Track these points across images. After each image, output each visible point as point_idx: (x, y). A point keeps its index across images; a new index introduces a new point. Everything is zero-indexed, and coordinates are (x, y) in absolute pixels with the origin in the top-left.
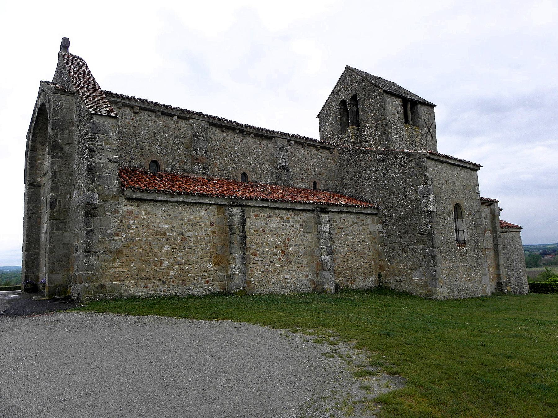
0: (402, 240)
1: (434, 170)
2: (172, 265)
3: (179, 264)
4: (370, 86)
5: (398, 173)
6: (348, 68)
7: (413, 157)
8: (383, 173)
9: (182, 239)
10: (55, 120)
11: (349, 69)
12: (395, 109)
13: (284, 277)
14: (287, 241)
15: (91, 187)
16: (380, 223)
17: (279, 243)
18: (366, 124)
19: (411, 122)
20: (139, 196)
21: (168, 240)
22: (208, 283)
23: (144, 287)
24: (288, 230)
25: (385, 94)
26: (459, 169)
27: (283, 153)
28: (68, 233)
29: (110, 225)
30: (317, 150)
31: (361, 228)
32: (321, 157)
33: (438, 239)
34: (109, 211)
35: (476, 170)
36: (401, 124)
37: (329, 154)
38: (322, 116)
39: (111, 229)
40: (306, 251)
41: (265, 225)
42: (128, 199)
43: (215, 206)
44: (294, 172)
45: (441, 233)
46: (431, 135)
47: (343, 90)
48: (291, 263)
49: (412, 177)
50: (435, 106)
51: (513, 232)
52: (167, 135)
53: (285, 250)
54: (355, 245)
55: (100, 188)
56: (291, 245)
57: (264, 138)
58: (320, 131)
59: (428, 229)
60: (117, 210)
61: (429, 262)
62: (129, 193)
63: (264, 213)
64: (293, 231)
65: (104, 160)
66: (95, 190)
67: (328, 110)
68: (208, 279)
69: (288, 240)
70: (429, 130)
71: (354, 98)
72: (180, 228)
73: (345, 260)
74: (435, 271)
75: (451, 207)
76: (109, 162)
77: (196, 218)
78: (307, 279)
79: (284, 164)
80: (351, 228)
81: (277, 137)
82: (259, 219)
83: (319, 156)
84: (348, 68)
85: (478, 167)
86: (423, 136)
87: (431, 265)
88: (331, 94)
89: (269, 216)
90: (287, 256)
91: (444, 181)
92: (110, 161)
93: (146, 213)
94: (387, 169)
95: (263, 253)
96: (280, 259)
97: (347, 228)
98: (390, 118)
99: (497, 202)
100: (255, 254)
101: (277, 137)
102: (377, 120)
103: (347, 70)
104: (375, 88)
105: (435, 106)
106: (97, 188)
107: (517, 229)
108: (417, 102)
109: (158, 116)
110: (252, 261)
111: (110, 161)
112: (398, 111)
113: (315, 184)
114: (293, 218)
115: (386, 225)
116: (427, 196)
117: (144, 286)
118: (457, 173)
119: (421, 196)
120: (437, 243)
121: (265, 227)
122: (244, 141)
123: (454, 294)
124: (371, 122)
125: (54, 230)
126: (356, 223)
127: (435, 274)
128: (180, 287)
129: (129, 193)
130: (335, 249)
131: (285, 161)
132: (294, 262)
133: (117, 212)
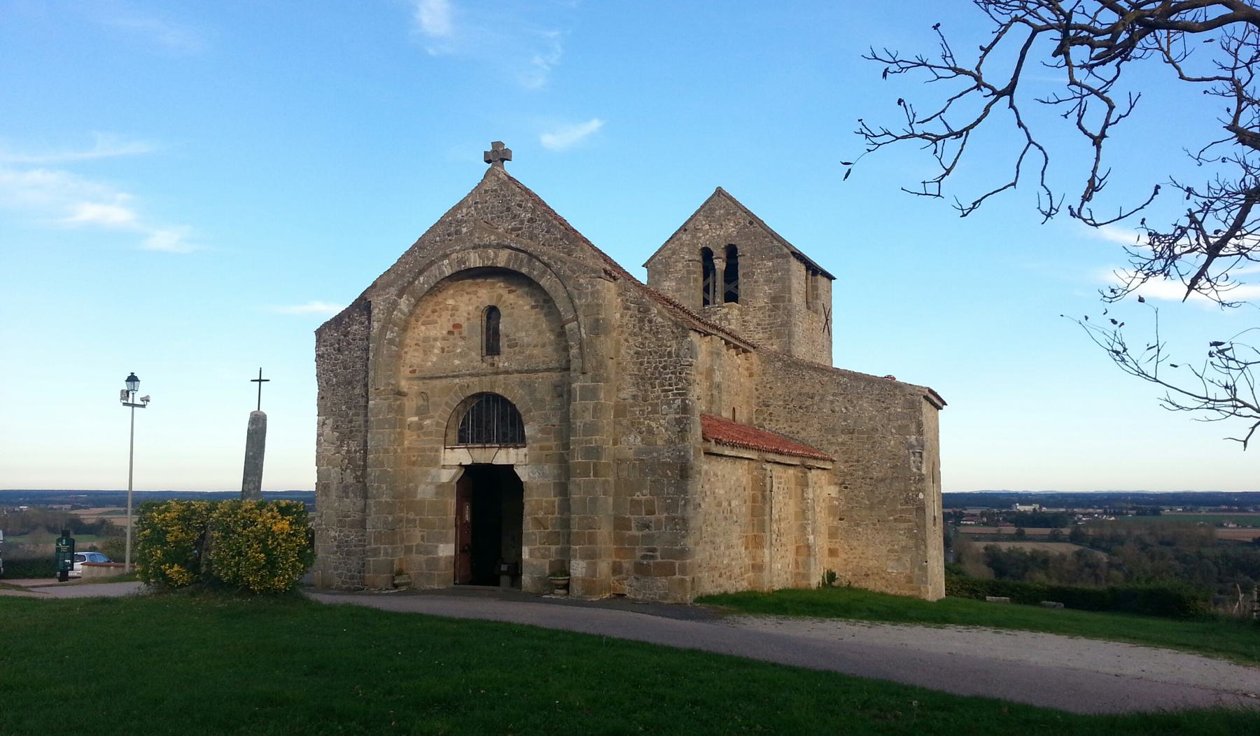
0: (873, 513)
4: (765, 237)
6: (719, 192)
8: (846, 408)
11: (723, 194)
16: (836, 484)
18: (751, 301)
25: (792, 257)
36: (804, 310)
42: (708, 453)
47: (708, 230)
50: (835, 279)
59: (920, 500)
61: (917, 547)
67: (670, 258)
74: (926, 562)
84: (719, 192)
88: (680, 230)
94: (852, 403)
103: (719, 196)
104: (775, 242)
105: (835, 279)
115: (846, 488)
119: (911, 451)
124: (762, 301)
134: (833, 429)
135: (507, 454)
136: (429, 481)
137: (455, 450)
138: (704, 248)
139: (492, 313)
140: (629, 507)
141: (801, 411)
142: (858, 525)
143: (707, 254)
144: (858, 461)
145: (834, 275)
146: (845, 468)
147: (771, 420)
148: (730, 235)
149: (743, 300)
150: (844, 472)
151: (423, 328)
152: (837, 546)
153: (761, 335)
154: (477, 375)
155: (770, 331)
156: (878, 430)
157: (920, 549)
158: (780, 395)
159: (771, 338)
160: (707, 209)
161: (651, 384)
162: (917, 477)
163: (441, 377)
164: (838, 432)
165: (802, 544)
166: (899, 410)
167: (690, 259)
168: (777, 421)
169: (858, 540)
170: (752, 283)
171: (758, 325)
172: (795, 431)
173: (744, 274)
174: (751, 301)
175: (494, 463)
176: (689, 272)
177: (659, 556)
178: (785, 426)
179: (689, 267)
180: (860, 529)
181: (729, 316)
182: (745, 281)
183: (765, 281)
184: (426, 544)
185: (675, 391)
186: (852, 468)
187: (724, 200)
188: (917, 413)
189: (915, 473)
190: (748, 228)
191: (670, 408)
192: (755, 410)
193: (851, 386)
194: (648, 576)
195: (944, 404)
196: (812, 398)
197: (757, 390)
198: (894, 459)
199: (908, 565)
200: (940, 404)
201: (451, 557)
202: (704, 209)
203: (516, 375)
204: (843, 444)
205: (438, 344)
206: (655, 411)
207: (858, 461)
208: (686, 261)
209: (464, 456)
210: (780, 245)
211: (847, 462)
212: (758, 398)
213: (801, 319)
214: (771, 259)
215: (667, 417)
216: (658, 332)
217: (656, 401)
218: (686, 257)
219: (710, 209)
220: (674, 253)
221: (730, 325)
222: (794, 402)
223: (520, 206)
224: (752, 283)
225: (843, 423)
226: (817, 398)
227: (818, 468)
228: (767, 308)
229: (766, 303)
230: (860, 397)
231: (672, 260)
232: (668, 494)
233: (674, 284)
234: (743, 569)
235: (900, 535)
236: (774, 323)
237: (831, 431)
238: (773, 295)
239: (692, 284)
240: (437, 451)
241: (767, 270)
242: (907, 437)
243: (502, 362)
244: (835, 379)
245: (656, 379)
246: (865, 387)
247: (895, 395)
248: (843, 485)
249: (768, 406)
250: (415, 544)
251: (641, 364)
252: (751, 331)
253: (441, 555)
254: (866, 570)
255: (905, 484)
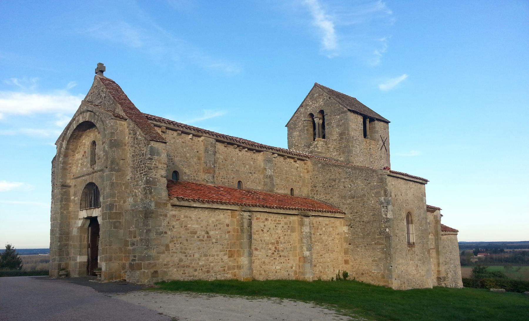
0: (364, 240)
1: (392, 185)
2: (201, 256)
3: (206, 255)
5: (363, 185)
6: (316, 85)
7: (376, 173)
8: (350, 185)
9: (208, 237)
10: (113, 141)
12: (357, 125)
13: (275, 268)
14: (279, 240)
15: (150, 196)
16: (347, 225)
17: (273, 241)
18: (331, 137)
19: (369, 136)
20: (183, 203)
21: (198, 237)
22: (224, 271)
23: (182, 273)
24: (279, 231)
26: (411, 184)
27: (270, 164)
28: (122, 230)
29: (161, 226)
30: (295, 162)
31: (331, 229)
32: (298, 167)
33: (395, 241)
34: (161, 215)
35: (424, 184)
37: (304, 165)
38: (291, 126)
39: (161, 229)
40: (291, 248)
41: (262, 226)
42: (173, 205)
43: (230, 211)
44: (277, 181)
45: (396, 236)
46: (386, 148)
47: (311, 105)
48: (281, 257)
49: (375, 189)
51: (451, 235)
52: (185, 150)
53: (277, 247)
54: (327, 243)
55: (155, 197)
56: (281, 242)
57: (255, 151)
58: (288, 138)
60: (166, 214)
61: (386, 258)
62: (175, 201)
63: (263, 216)
64: (283, 231)
65: (158, 176)
66: (152, 199)
67: (296, 121)
68: (224, 268)
69: (279, 238)
70: (384, 144)
71: (322, 112)
72: (207, 228)
73: (319, 255)
74: (392, 267)
75: (404, 215)
76: (161, 177)
77: (217, 220)
78: (292, 270)
79: (270, 174)
80: (324, 229)
81: (265, 151)
82: (260, 221)
83: (296, 166)
84: (316, 85)
85: (424, 182)
86: (379, 149)
87: (388, 261)
88: (300, 107)
89: (267, 219)
90: (278, 251)
91: (399, 194)
92: (162, 176)
93: (185, 217)
94: (353, 182)
95: (262, 248)
96: (273, 254)
97: (322, 229)
98: (352, 133)
99: (439, 209)
100: (256, 249)
101: (265, 151)
102: (341, 134)
104: (341, 106)
105: (390, 122)
106: (153, 197)
107: (455, 232)
108: (375, 119)
109: (179, 135)
110: (254, 255)
111: (162, 176)
112: (359, 127)
113: (292, 189)
114: (283, 221)
115: (351, 227)
116: (387, 206)
117: (183, 272)
118: (410, 187)
119: (382, 206)
120: (393, 245)
121: (264, 228)
122: (240, 154)
123: (405, 285)
124: (335, 136)
125: (112, 228)
126: (328, 225)
127: (391, 268)
128: (206, 274)
129: (175, 201)
130: (312, 246)
131: (271, 171)
132: (283, 256)
133: (166, 216)
134: (345, 196)
135: (96, 211)
136: (76, 226)
137: (83, 211)
138: (310, 114)
139: (94, 143)
140: (128, 234)
141: (330, 188)
142: (357, 247)
143: (311, 115)
144: (357, 213)
145: (389, 120)
146: (351, 216)
147: (317, 194)
148: (321, 106)
149: (327, 137)
150: (351, 219)
151: (77, 155)
152: (348, 259)
153: (336, 153)
154: (88, 174)
155: (340, 151)
156: (366, 195)
157: (388, 260)
158: (321, 181)
159: (340, 154)
160: (311, 95)
161: (137, 170)
162: (385, 220)
163: (79, 177)
164: (347, 198)
165: (301, 256)
166: (375, 184)
167: (305, 120)
168: (320, 194)
169: (358, 255)
170: (331, 128)
171: (334, 148)
172: (328, 199)
173: (327, 124)
174: (331, 137)
175: (93, 216)
176: (304, 126)
177: (137, 259)
178: (324, 196)
179: (304, 124)
180: (359, 249)
181: (318, 145)
182: (328, 127)
183: (337, 126)
184: (75, 256)
185: (144, 173)
186: (354, 217)
187: (318, 89)
188: (384, 185)
189: (384, 218)
190: (328, 100)
191: (142, 182)
192: (310, 190)
193: (352, 173)
194: (133, 270)
195: (427, 181)
196: (335, 181)
197: (311, 179)
198: (374, 210)
199: (382, 268)
200: (424, 182)
201: (84, 262)
202: (309, 95)
203: (99, 173)
204: (350, 204)
205: (80, 162)
206: (137, 185)
207: (357, 213)
208: (303, 121)
209: (84, 214)
210: (342, 107)
211: (351, 213)
212: (312, 183)
213: (358, 143)
214: (339, 115)
215: (141, 186)
216: (139, 144)
217: (138, 179)
218: (303, 119)
219: (312, 94)
220: (298, 118)
221: (318, 149)
222: (327, 184)
223: (102, 91)
224: (331, 128)
225: (349, 193)
226: (337, 181)
227: (313, 216)
228: (338, 139)
229: (337, 137)
230: (356, 179)
231: (297, 121)
232: (141, 227)
233: (298, 133)
234: (226, 269)
235: (378, 252)
236: (341, 147)
237: (344, 197)
238: (340, 133)
239: (305, 132)
240: (78, 212)
241: (337, 120)
242: (380, 198)
243: (96, 168)
244: (345, 170)
245: (138, 168)
246: (359, 173)
247: (373, 176)
248: (350, 226)
249: (316, 187)
250: (72, 256)
251: (134, 161)
252: (331, 152)
253: (78, 261)
254: (362, 271)
255: (379, 224)
